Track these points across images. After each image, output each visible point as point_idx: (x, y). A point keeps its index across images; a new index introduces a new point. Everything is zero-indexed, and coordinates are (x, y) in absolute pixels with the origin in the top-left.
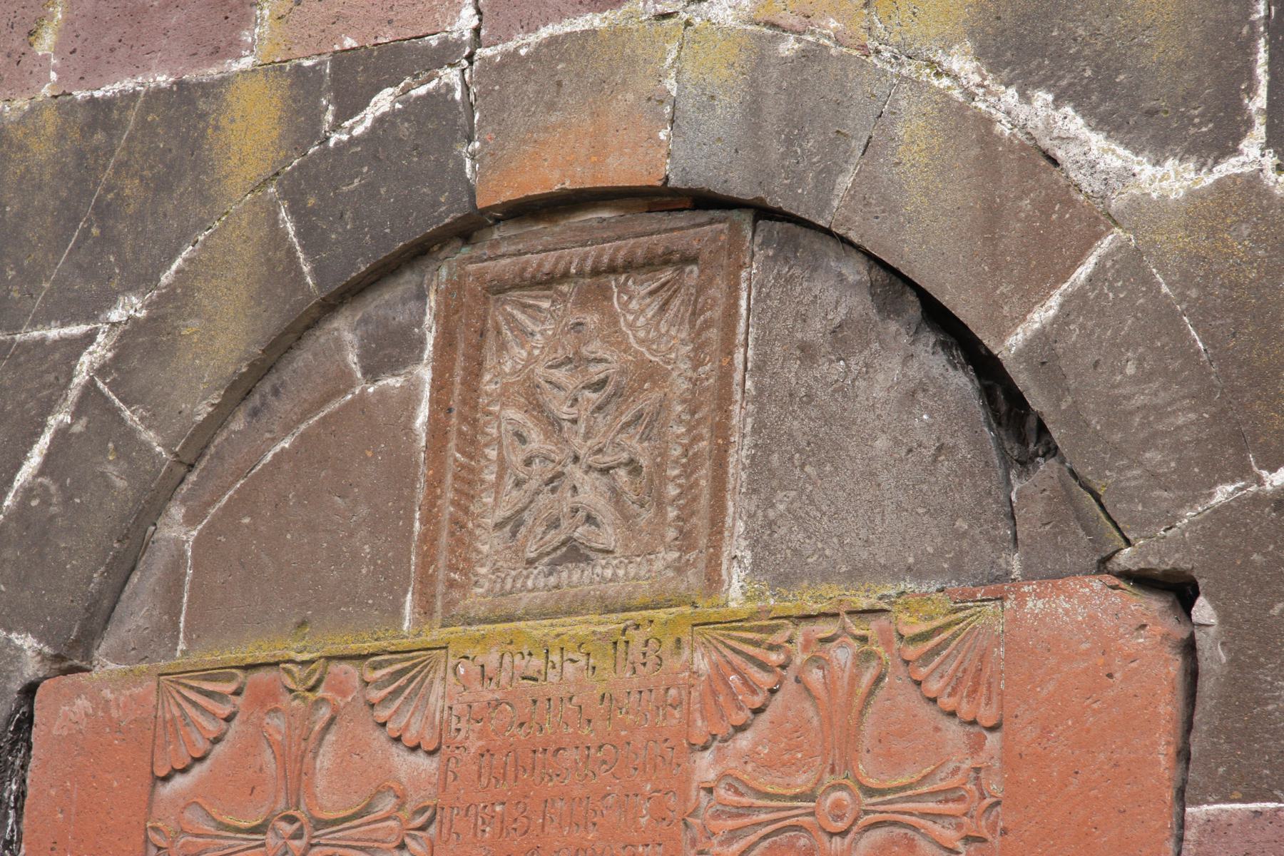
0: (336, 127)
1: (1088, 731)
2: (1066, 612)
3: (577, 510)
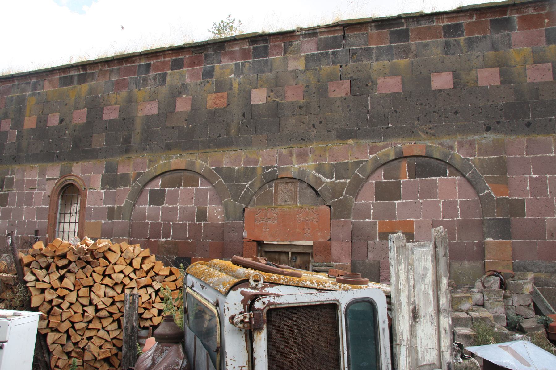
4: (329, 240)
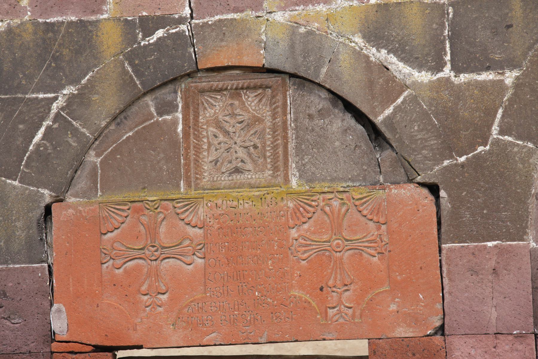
0: (143, 39)
1: (413, 225)
2: (404, 193)
3: (238, 158)
4: (436, 333)
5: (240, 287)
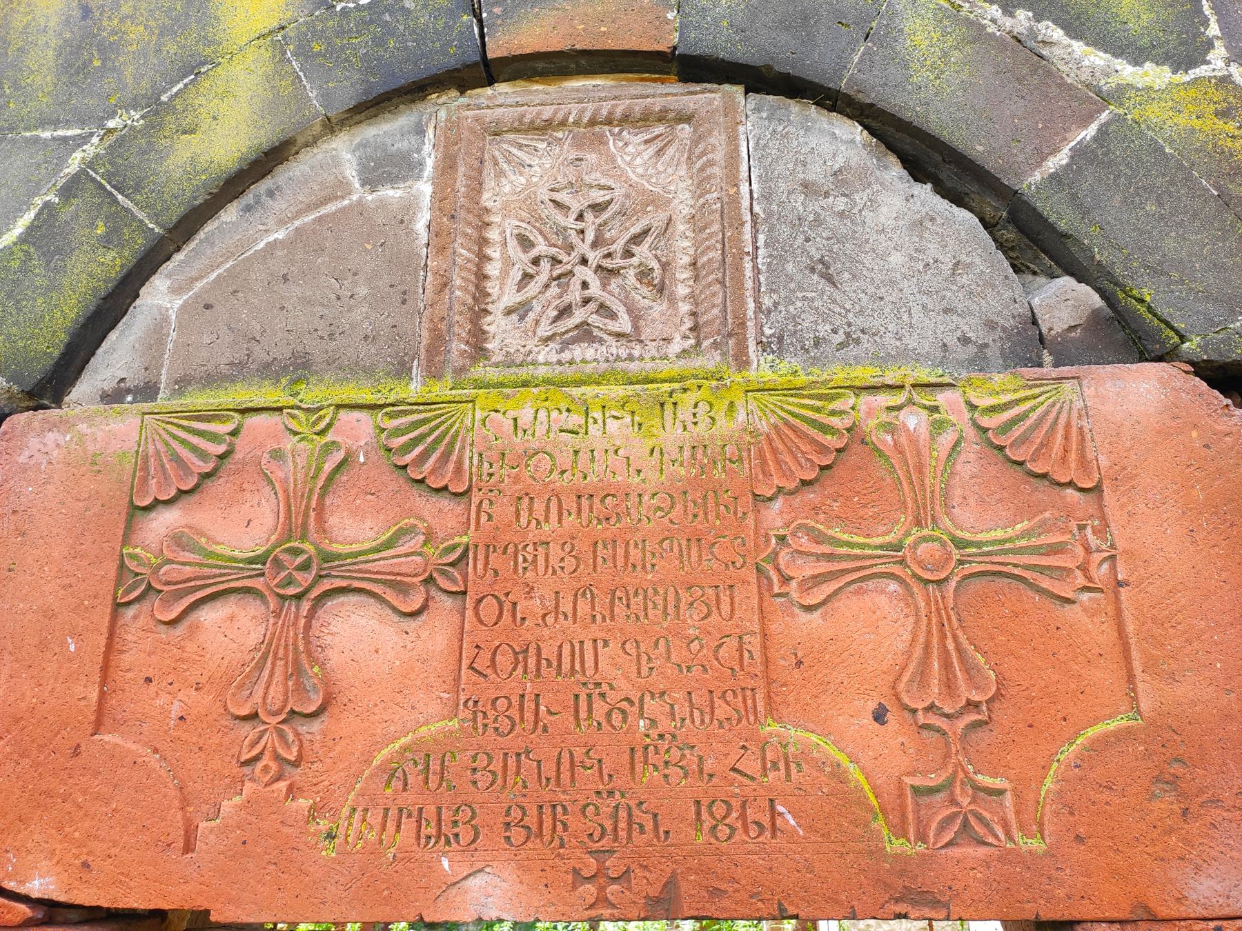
5: (583, 697)
